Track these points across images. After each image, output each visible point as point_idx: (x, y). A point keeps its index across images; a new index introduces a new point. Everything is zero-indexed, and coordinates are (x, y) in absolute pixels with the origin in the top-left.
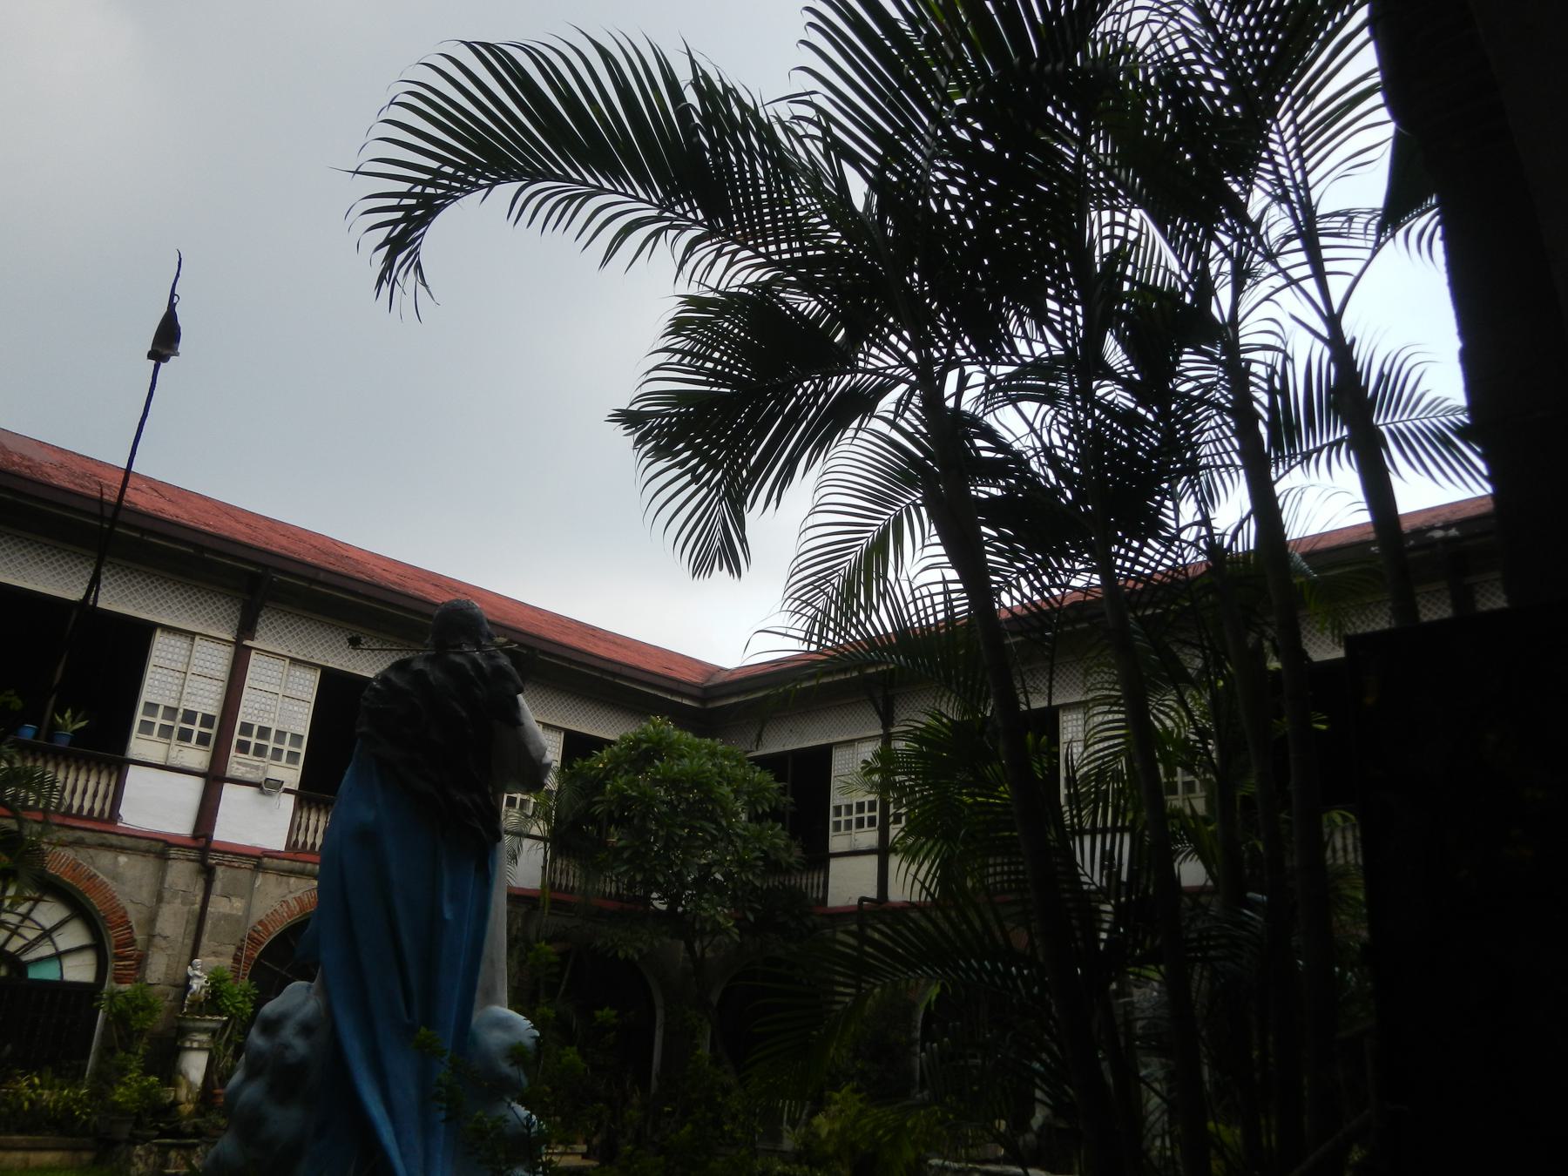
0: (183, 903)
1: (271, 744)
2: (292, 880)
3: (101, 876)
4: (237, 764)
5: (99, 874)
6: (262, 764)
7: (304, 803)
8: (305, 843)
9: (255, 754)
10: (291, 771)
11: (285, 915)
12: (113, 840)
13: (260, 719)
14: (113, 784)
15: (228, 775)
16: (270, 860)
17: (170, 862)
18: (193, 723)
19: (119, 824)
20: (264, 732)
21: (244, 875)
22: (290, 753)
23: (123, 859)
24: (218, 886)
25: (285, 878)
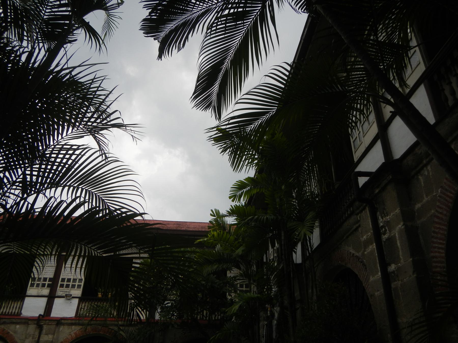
0: (33, 338)
2: (73, 327)
3: (11, 333)
4: (60, 291)
5: (10, 331)
6: (68, 290)
10: (79, 291)
11: (70, 339)
12: (14, 321)
13: (68, 276)
14: (22, 303)
15: (57, 295)
16: (64, 321)
17: (29, 325)
19: (21, 316)
20: (69, 280)
21: (53, 327)
23: (18, 326)
24: (44, 331)
25: (70, 327)
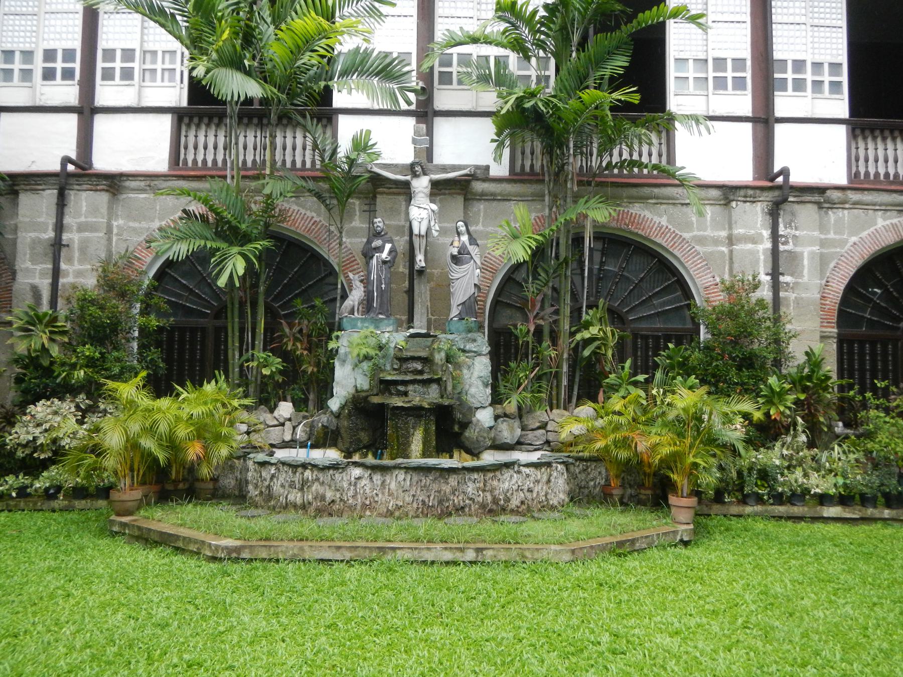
1: (809, 76)
7: (858, 132)
8: (867, 174)
9: (795, 90)
18: (725, 70)
22: (831, 83)
